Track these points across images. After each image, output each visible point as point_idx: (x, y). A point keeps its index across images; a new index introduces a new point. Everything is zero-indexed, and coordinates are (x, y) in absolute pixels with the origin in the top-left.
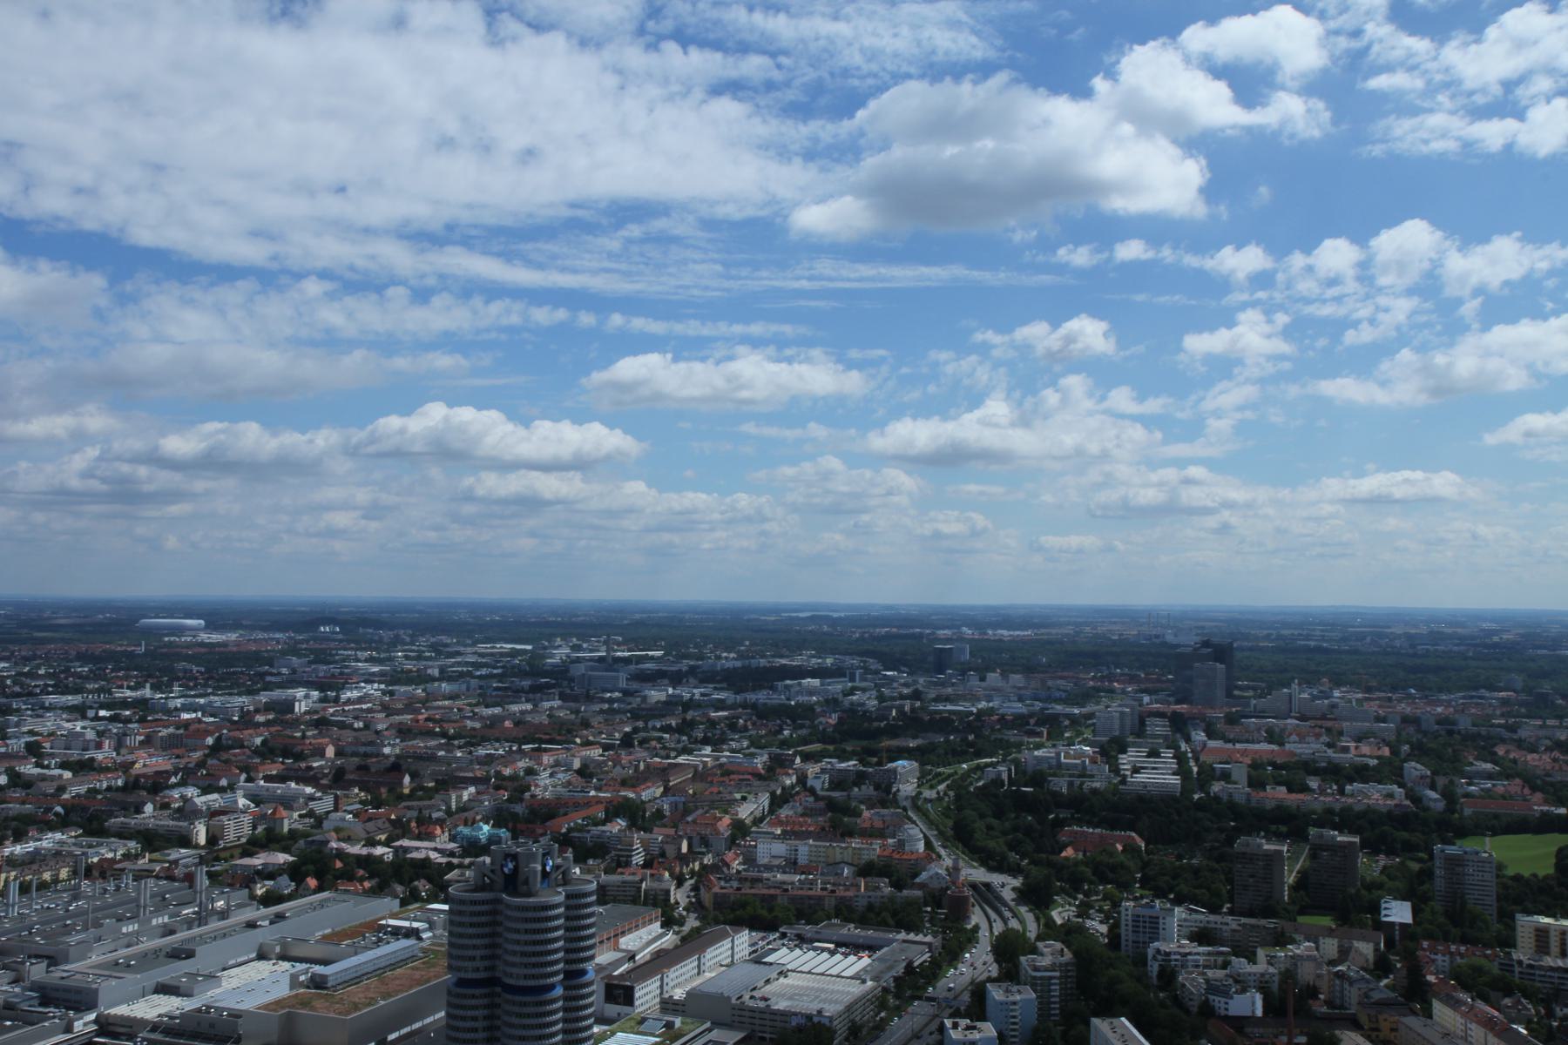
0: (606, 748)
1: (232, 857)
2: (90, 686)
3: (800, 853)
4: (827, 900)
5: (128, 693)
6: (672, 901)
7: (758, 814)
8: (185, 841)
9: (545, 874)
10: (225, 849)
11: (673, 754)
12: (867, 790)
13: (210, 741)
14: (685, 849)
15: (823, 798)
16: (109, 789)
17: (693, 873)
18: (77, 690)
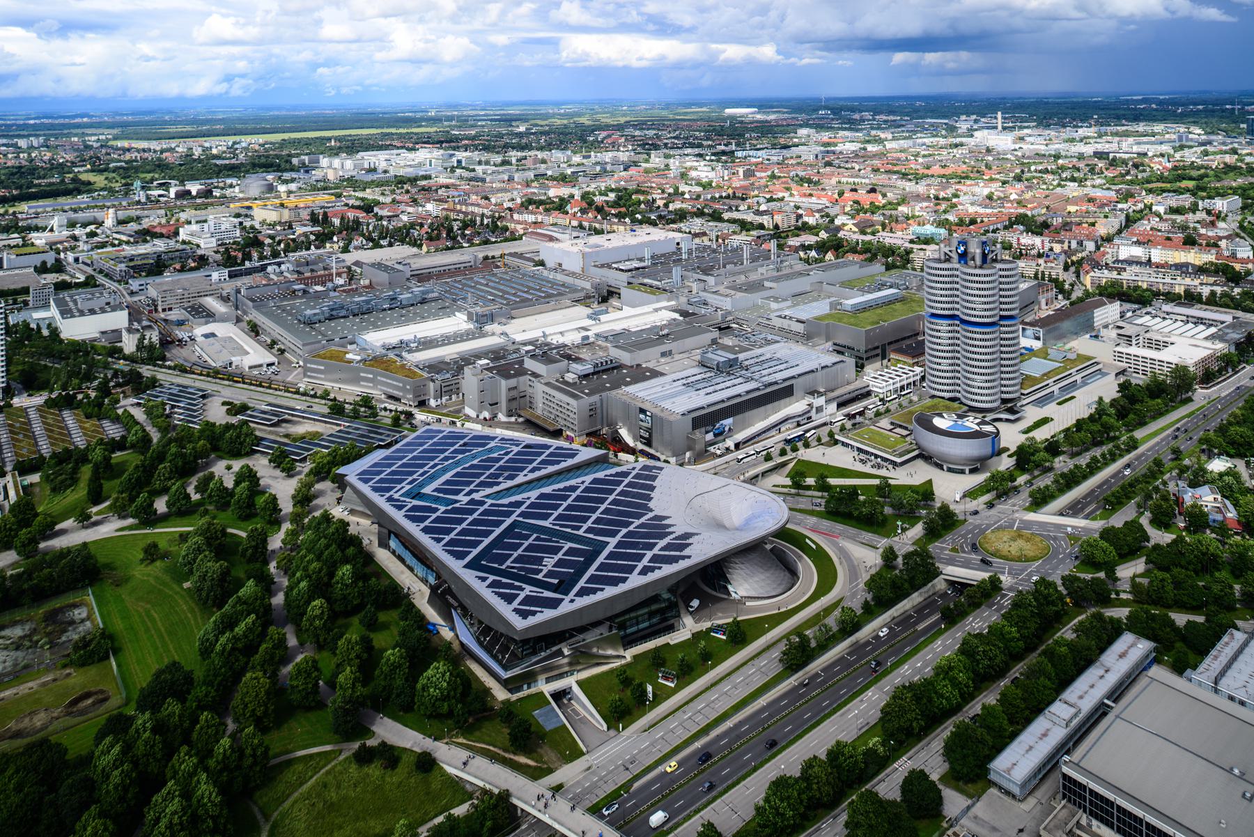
0: (1004, 183)
1: (788, 236)
2: (705, 143)
3: (1152, 254)
4: (1177, 286)
5: (723, 147)
6: (1061, 279)
7: (1117, 227)
8: (761, 226)
9: (984, 256)
10: (783, 232)
11: (1051, 187)
12: (1201, 215)
13: (769, 173)
14: (1066, 246)
15: (1166, 220)
16: (721, 197)
17: (1073, 263)
18: (700, 146)
